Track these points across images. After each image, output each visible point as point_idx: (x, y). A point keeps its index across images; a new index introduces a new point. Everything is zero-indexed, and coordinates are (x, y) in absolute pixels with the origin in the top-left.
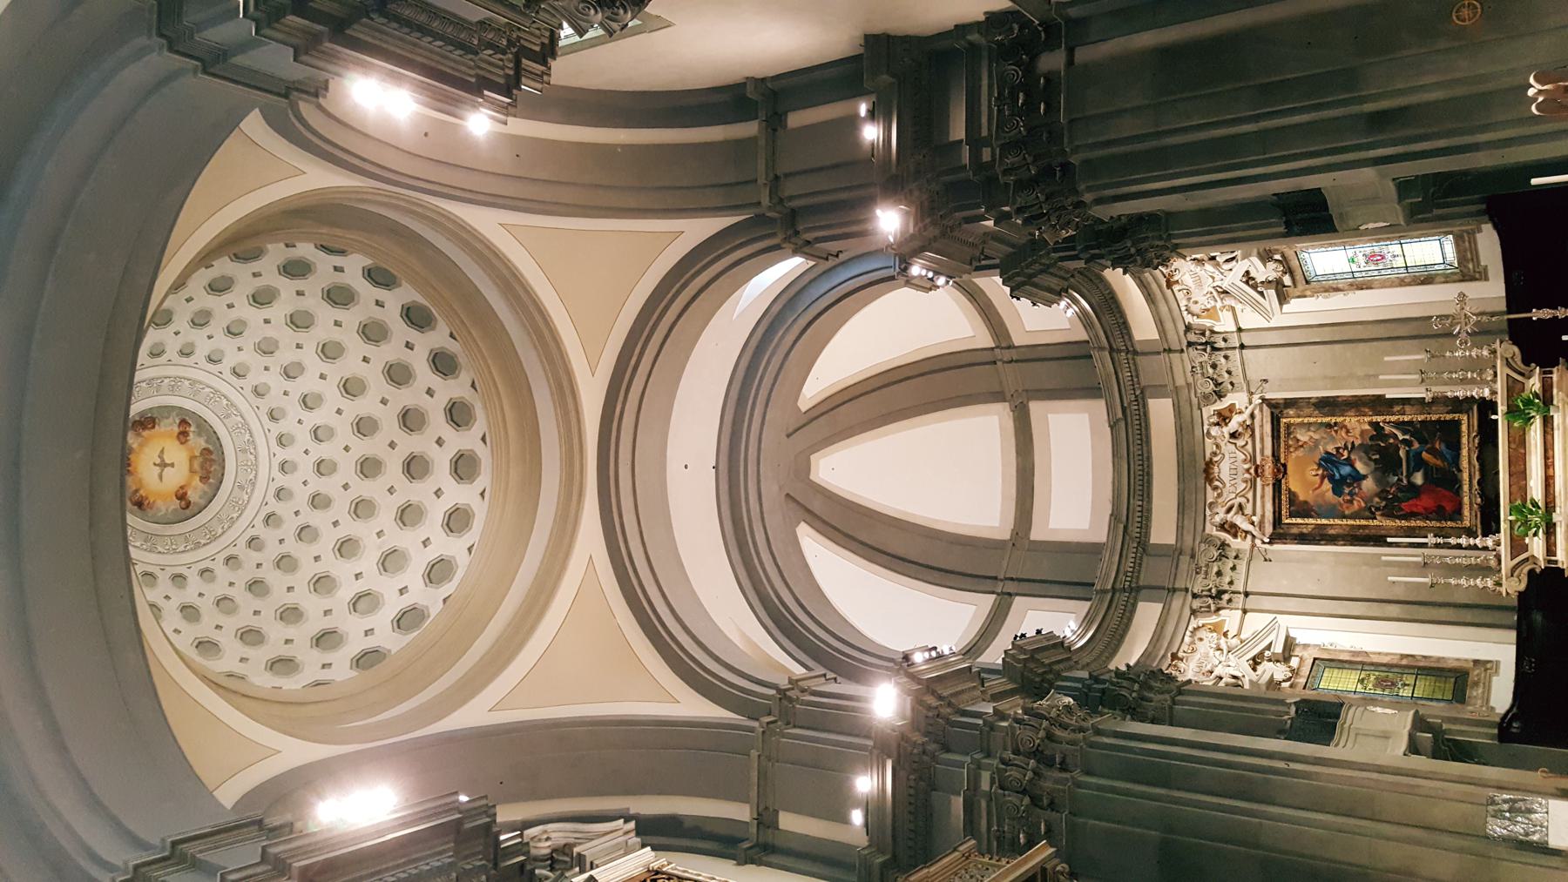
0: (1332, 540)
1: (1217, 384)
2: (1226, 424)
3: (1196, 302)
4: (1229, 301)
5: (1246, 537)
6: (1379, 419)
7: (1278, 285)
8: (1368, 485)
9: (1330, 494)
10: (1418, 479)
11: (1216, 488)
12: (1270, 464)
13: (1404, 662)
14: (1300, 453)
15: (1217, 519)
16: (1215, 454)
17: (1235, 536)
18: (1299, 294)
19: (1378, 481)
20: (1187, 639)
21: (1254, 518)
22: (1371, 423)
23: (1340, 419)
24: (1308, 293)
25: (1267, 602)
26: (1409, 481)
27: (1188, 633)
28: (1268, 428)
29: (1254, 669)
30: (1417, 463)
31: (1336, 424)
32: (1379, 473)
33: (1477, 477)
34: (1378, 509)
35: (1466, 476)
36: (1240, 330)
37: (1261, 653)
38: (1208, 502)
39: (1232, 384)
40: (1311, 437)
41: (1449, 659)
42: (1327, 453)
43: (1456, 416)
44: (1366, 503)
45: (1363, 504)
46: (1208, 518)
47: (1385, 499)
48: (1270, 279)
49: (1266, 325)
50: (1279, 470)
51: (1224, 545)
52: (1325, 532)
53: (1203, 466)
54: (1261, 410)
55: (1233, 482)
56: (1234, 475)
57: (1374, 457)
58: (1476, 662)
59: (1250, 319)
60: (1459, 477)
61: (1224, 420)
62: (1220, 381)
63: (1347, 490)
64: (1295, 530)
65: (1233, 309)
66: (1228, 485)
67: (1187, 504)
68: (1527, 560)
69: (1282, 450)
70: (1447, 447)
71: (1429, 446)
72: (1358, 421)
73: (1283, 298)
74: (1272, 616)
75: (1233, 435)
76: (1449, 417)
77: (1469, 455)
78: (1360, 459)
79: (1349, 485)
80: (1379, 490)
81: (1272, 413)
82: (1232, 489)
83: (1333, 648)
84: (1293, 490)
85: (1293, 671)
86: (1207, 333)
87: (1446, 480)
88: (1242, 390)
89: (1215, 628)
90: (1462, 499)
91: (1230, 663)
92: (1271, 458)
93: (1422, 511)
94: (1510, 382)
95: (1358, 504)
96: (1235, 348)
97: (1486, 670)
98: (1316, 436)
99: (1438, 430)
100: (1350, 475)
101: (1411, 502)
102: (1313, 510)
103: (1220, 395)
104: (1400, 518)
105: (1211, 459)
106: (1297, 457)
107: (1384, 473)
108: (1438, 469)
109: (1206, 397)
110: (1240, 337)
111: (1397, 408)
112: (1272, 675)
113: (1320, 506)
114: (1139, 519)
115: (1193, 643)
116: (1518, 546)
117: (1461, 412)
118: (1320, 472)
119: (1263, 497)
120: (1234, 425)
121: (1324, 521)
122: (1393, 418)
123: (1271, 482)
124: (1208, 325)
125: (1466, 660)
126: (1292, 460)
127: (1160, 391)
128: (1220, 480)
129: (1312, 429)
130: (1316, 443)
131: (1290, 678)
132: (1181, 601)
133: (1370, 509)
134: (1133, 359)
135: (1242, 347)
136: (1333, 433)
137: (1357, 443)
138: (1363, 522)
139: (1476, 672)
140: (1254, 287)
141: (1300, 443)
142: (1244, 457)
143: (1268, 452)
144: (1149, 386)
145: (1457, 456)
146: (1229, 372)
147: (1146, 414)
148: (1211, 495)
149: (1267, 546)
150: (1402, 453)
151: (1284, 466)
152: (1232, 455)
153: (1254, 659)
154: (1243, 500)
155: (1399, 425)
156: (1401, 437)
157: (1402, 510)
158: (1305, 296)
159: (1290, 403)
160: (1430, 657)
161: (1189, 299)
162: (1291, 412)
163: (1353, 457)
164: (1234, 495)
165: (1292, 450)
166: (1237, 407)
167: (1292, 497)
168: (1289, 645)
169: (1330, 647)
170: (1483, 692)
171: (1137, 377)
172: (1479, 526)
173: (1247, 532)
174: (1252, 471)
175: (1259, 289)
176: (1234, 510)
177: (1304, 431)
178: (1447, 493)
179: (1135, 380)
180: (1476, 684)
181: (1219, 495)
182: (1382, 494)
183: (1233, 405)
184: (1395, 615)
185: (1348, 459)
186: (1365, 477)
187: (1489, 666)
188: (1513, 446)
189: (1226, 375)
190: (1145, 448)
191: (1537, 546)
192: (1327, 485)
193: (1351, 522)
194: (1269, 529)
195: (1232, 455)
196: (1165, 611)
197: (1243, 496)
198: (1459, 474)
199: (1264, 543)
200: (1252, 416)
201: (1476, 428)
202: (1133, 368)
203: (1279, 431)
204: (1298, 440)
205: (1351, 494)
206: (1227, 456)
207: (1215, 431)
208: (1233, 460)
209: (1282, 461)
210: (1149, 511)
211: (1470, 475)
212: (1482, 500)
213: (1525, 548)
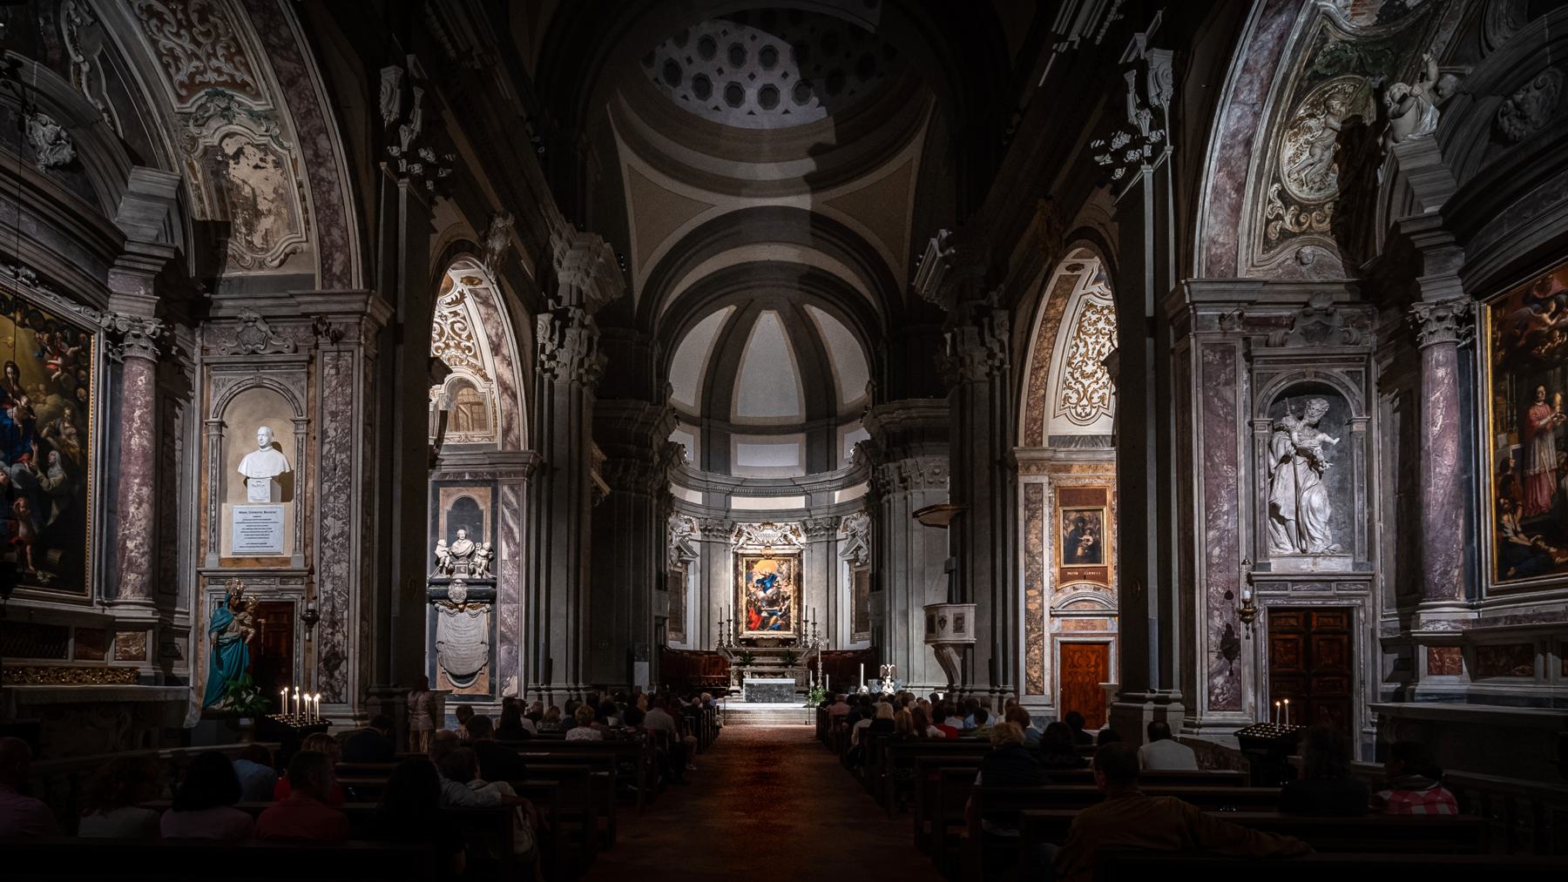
0: (736, 578)
8: (761, 594)
9: (755, 579)
10: (764, 614)
19: (763, 598)
64: (740, 563)
87: (764, 625)
95: (753, 590)
104: (747, 608)
154: (753, 537)
167: (756, 562)
182: (758, 600)
192: (761, 577)
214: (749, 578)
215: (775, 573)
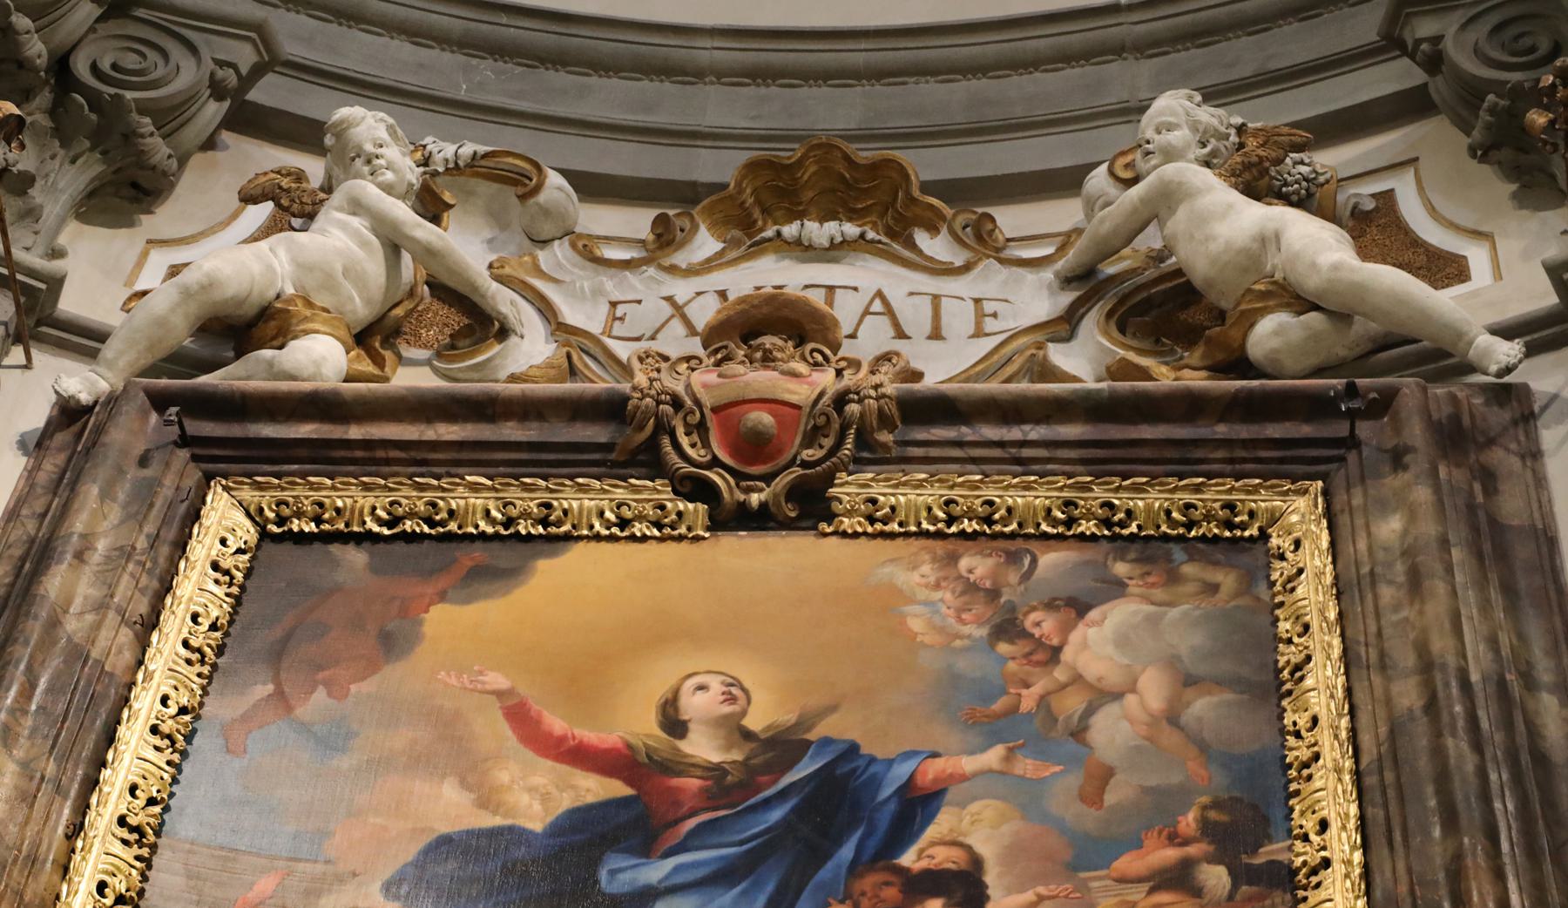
40: (1103, 695)
204: (1078, 607)
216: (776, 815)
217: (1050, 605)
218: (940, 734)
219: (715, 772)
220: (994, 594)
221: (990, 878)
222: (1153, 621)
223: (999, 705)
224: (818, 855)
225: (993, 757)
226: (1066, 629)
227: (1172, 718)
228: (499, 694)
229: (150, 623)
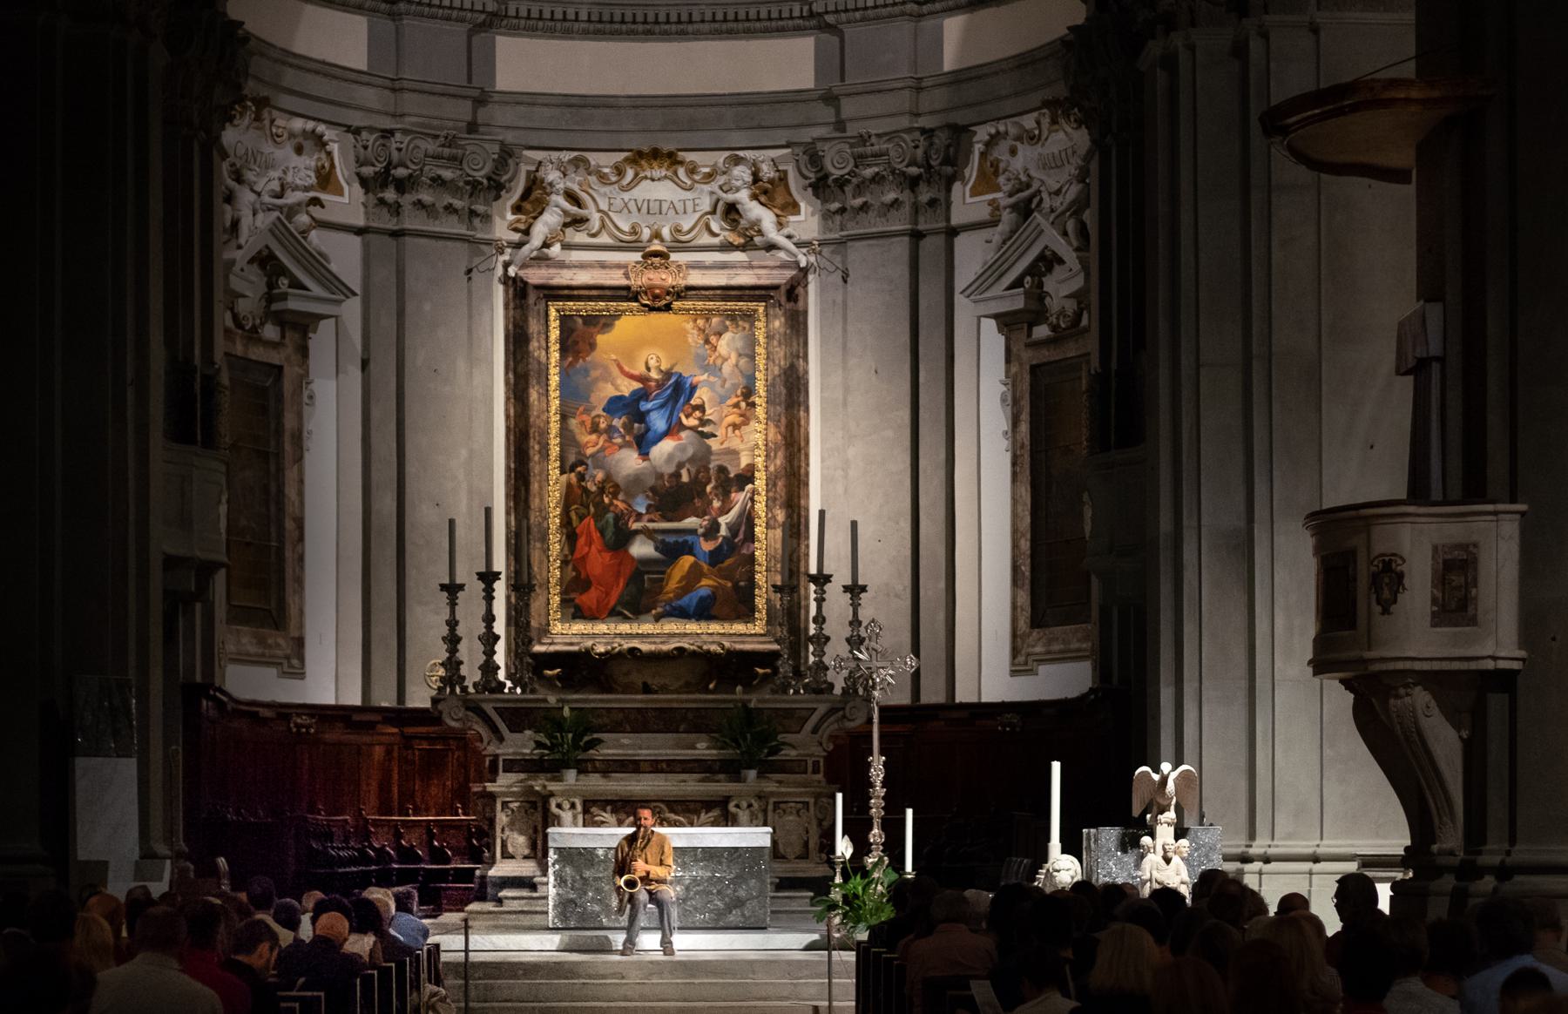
1: (841, 183)
2: (754, 197)
3: (1013, 152)
4: (1007, 217)
5: (516, 230)
6: (760, 482)
7: (1035, 312)
8: (629, 462)
9: (609, 391)
10: (641, 549)
11: (620, 172)
12: (670, 281)
13: (289, 525)
14: (694, 338)
15: (552, 176)
16: (692, 171)
17: (517, 209)
18: (1014, 350)
19: (636, 480)
20: (298, 124)
21: (556, 250)
22: (751, 468)
23: (760, 412)
24: (1014, 369)
25: (384, 274)
26: (637, 532)
27: (310, 125)
28: (745, 278)
29: (251, 261)
30: (672, 550)
31: (753, 405)
32: (651, 482)
33: (645, 647)
34: (581, 477)
35: (647, 627)
36: (952, 232)
37: (283, 271)
38: (587, 155)
39: (842, 210)
40: (725, 360)
41: (302, 598)
42: (693, 388)
43: (761, 615)
44: (592, 456)
45: (589, 451)
46: (555, 155)
47: (602, 490)
48: (1048, 300)
49: (961, 283)
50: (656, 297)
51: (496, 188)
52: (533, 381)
53: (666, 147)
54: (784, 266)
55: (632, 206)
56: (652, 209)
57: (684, 473)
58: (300, 643)
59: (971, 255)
60: (642, 617)
61: (765, 192)
62: (848, 189)
63: (618, 423)
64: (534, 326)
65: (993, 223)
66: (626, 196)
67: (586, 111)
68: (494, 729)
69: (700, 304)
70: (702, 599)
71: (706, 567)
72: (757, 446)
73: (1006, 322)
74: (356, 286)
75: (731, 212)
76: (760, 602)
77: (685, 635)
78: (682, 449)
79: (628, 427)
80: (620, 480)
81: (776, 287)
82: (618, 203)
83: (306, 399)
84: (617, 323)
85: (254, 329)
86: (949, 170)
88: (826, 228)
89: (325, 179)
90: (603, 620)
91: (260, 216)
92: (683, 283)
93: (578, 555)
94: (804, 713)
95: (591, 443)
96: (916, 223)
97: (288, 658)
98: (727, 368)
99: (736, 586)
100: (648, 430)
101: (596, 535)
102: (576, 359)
103: (821, 187)
104: (566, 522)
105: (681, 163)
106: (684, 333)
107: (653, 489)
108: (660, 584)
109: (815, 159)
110: (935, 232)
111: (781, 515)
112: (244, 296)
113: (586, 372)
114: (547, 15)
115: (292, 135)
116: (518, 717)
117: (769, 623)
118: (654, 375)
119: (603, 265)
120: (755, 211)
121: (554, 380)
122: (760, 508)
123: (636, 282)
124: (967, 172)
125: (301, 626)
126: (679, 324)
127: (833, 64)
128: (637, 179)
129: (743, 361)
130: (715, 370)
131: (239, 325)
132: (376, 106)
133: (582, 463)
134: (903, 14)
135: (916, 236)
136: (735, 400)
137: (714, 444)
138: (555, 451)
139: (281, 641)
140: (1031, 270)
141: (713, 339)
142: (686, 227)
143: (696, 278)
144: (842, 41)
145: (683, 614)
146: (865, 207)
147: (781, 32)
148: (604, 161)
149: (499, 271)
150: (691, 522)
151: (668, 308)
152: (689, 205)
153: (272, 257)
154: (595, 223)
155: (748, 519)
156: (723, 520)
157: (581, 518)
158: (1008, 361)
159: (797, 323)
160: (302, 568)
161: (1019, 138)
162: (777, 324)
163: (684, 434)
164: (604, 206)
165: (700, 322)
166: (792, 218)
167: (604, 322)
168: (302, 326)
169: (306, 394)
170: (248, 654)
171: (863, 19)
172: (552, 648)
173: (527, 232)
174: (656, 246)
175: (1028, 279)
176: (574, 209)
177: (739, 344)
178: (613, 601)
179: (858, 15)
180: (261, 641)
181: (603, 178)
182: (611, 485)
183: (793, 207)
184: (375, 506)
185: (683, 427)
186: (644, 455)
187: (295, 662)
188: (690, 716)
189: (858, 201)
190: (706, 27)
191: (522, 744)
192: (627, 387)
193: (554, 428)
194: (535, 276)
195: (689, 205)
196: (353, 76)
197: (603, 226)
198: (649, 617)
199: (506, 265)
200: (771, 247)
201: (739, 647)
202: (884, 11)
203: (739, 299)
204: (720, 334)
205: (610, 429)
206: (689, 195)
207: (742, 173)
208: (680, 207)
209: (676, 305)
210: (567, 34)
211: (648, 635)
212: (600, 654)
213: (515, 728)
214: (573, 396)
215: (689, 371)
216: (669, 391)
217: (715, 334)
218: (697, 371)
219: (657, 381)
220: (704, 331)
221: (706, 406)
222: (733, 338)
223: (706, 362)
224: (677, 402)
225: (705, 376)
226: (718, 341)
227: (737, 365)
228: (615, 360)
229: (548, 348)
